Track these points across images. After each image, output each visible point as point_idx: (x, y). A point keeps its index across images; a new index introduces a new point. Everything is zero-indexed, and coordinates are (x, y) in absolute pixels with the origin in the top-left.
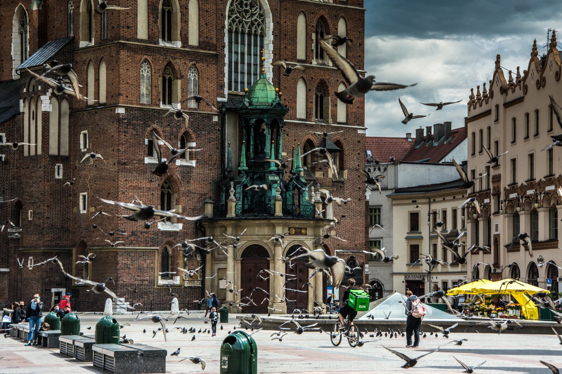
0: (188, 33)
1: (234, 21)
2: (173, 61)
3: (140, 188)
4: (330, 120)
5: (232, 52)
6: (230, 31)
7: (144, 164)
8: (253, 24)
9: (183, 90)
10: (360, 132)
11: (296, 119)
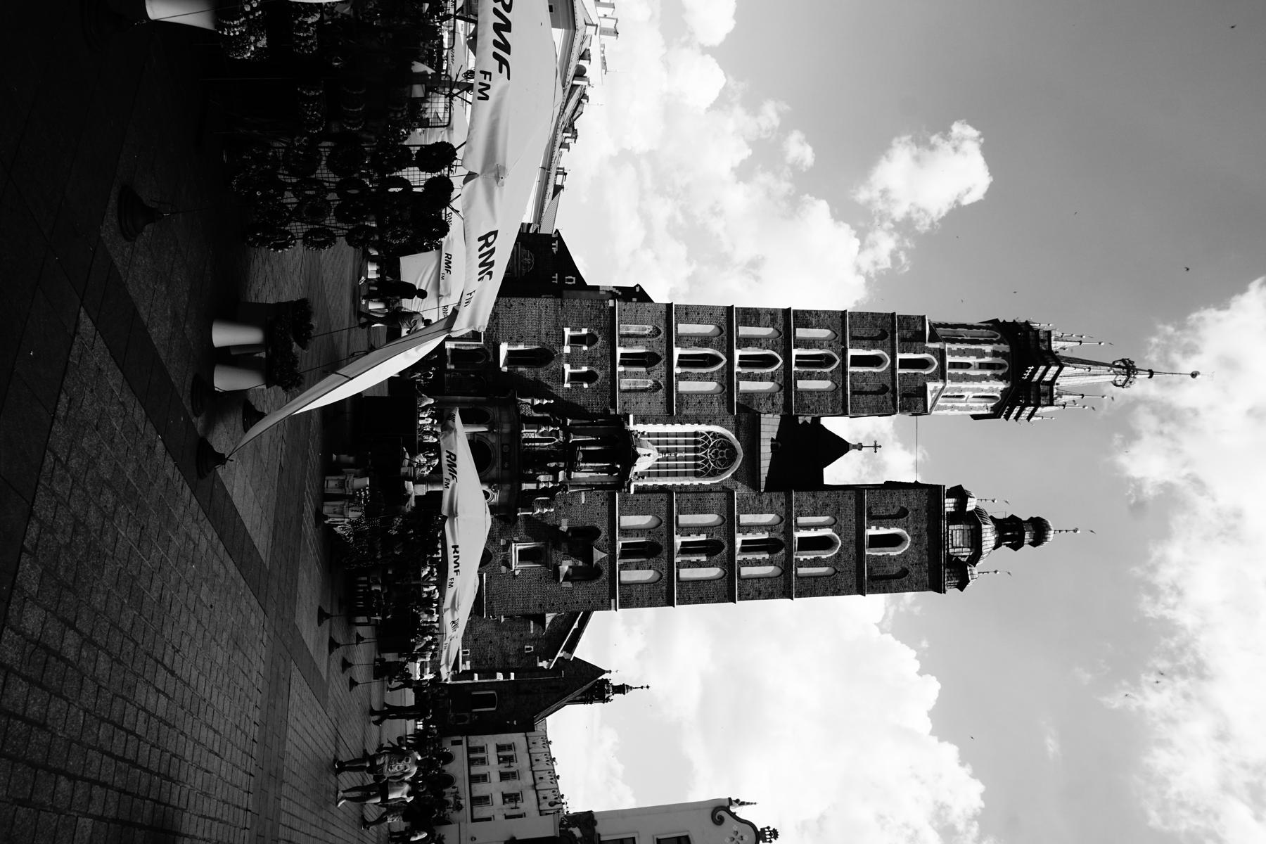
0: (689, 380)
1: (706, 438)
2: (662, 362)
3: (540, 321)
4: (623, 561)
5: (677, 437)
6: (696, 434)
7: (563, 327)
8: (706, 462)
9: (636, 373)
10: (613, 601)
11: (620, 515)
